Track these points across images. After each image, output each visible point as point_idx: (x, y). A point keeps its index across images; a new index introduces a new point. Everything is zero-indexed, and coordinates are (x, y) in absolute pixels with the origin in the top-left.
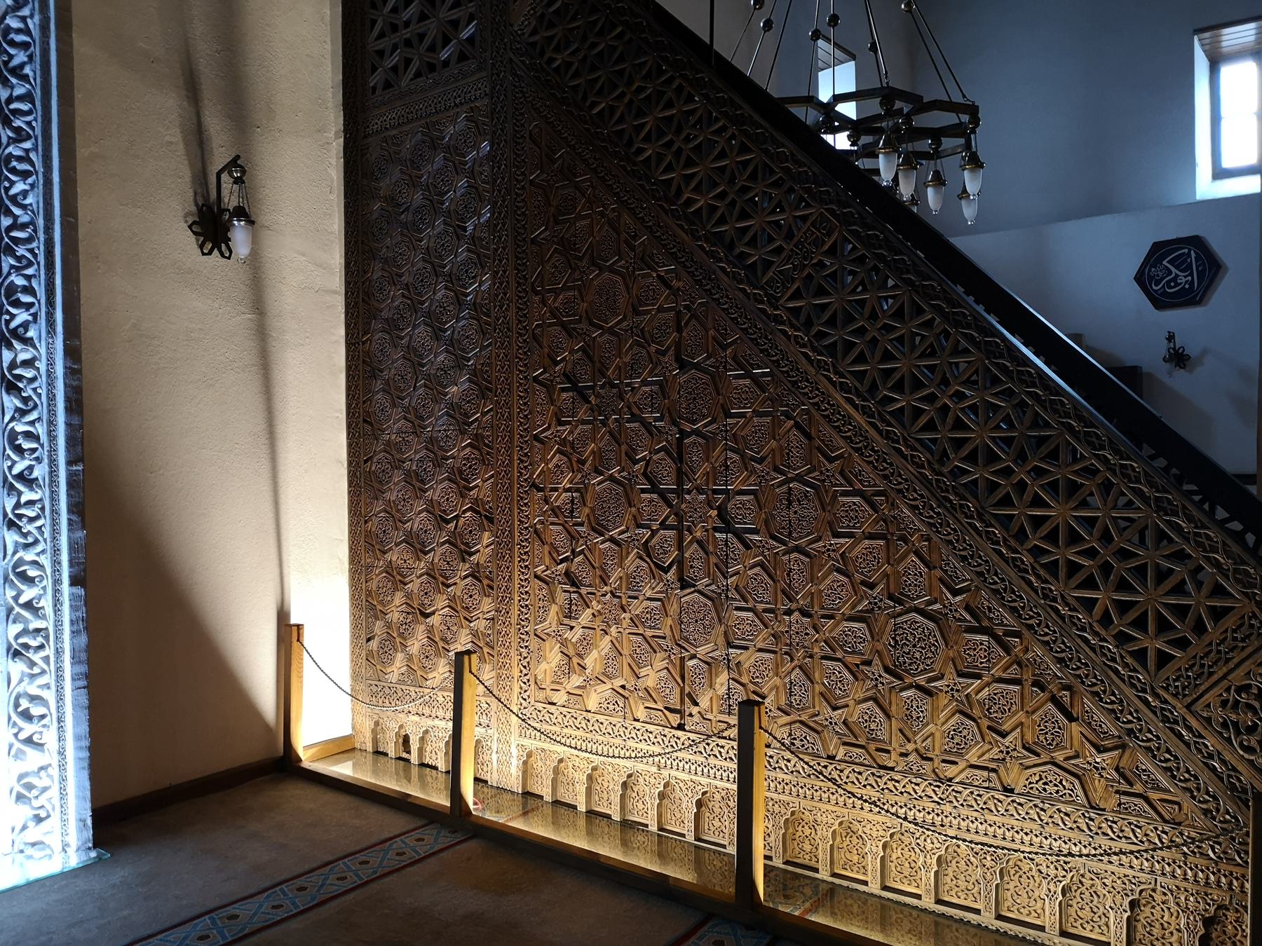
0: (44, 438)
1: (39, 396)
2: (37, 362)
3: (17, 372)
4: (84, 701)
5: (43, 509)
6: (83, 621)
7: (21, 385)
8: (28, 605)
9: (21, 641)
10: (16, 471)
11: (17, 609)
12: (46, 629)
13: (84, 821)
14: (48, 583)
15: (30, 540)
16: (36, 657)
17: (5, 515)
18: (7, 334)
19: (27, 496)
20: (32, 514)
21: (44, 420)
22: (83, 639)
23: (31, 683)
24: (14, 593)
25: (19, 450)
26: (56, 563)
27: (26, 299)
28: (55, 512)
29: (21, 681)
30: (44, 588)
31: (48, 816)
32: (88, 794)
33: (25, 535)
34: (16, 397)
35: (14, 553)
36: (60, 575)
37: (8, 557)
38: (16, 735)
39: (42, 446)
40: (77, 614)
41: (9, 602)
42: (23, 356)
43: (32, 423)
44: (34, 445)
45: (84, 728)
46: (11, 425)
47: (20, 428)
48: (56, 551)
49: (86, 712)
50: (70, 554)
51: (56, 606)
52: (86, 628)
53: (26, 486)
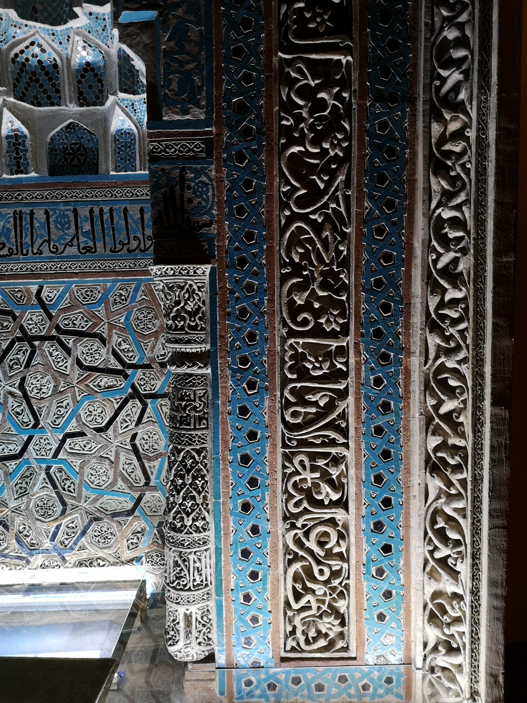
0: (471, 224)
1: (467, 172)
2: (468, 130)
3: (447, 147)
4: (503, 543)
5: (466, 310)
6: (505, 448)
7: (449, 163)
8: (448, 417)
9: (439, 454)
10: (440, 265)
11: (437, 420)
12: (465, 448)
13: (496, 682)
14: (468, 396)
15: (453, 345)
16: (455, 478)
17: (428, 314)
18: (437, 104)
19: (452, 294)
20: (455, 315)
21: (472, 201)
22: (505, 471)
23: (447, 503)
24: (434, 402)
25: (445, 241)
26: (478, 375)
28: (480, 314)
29: (438, 497)
30: (464, 402)
31: (458, 650)
32: (502, 648)
33: (447, 339)
34: (444, 178)
35: (437, 358)
36: (482, 390)
37: (430, 362)
38: (431, 552)
39: (468, 233)
40: (499, 440)
41: (429, 410)
42: (454, 126)
43: (458, 207)
44: (461, 234)
45: (500, 574)
46: (438, 212)
47: (447, 214)
48: (479, 362)
49: (504, 556)
50: (493, 366)
51: (476, 426)
52: (508, 458)
53: (449, 283)
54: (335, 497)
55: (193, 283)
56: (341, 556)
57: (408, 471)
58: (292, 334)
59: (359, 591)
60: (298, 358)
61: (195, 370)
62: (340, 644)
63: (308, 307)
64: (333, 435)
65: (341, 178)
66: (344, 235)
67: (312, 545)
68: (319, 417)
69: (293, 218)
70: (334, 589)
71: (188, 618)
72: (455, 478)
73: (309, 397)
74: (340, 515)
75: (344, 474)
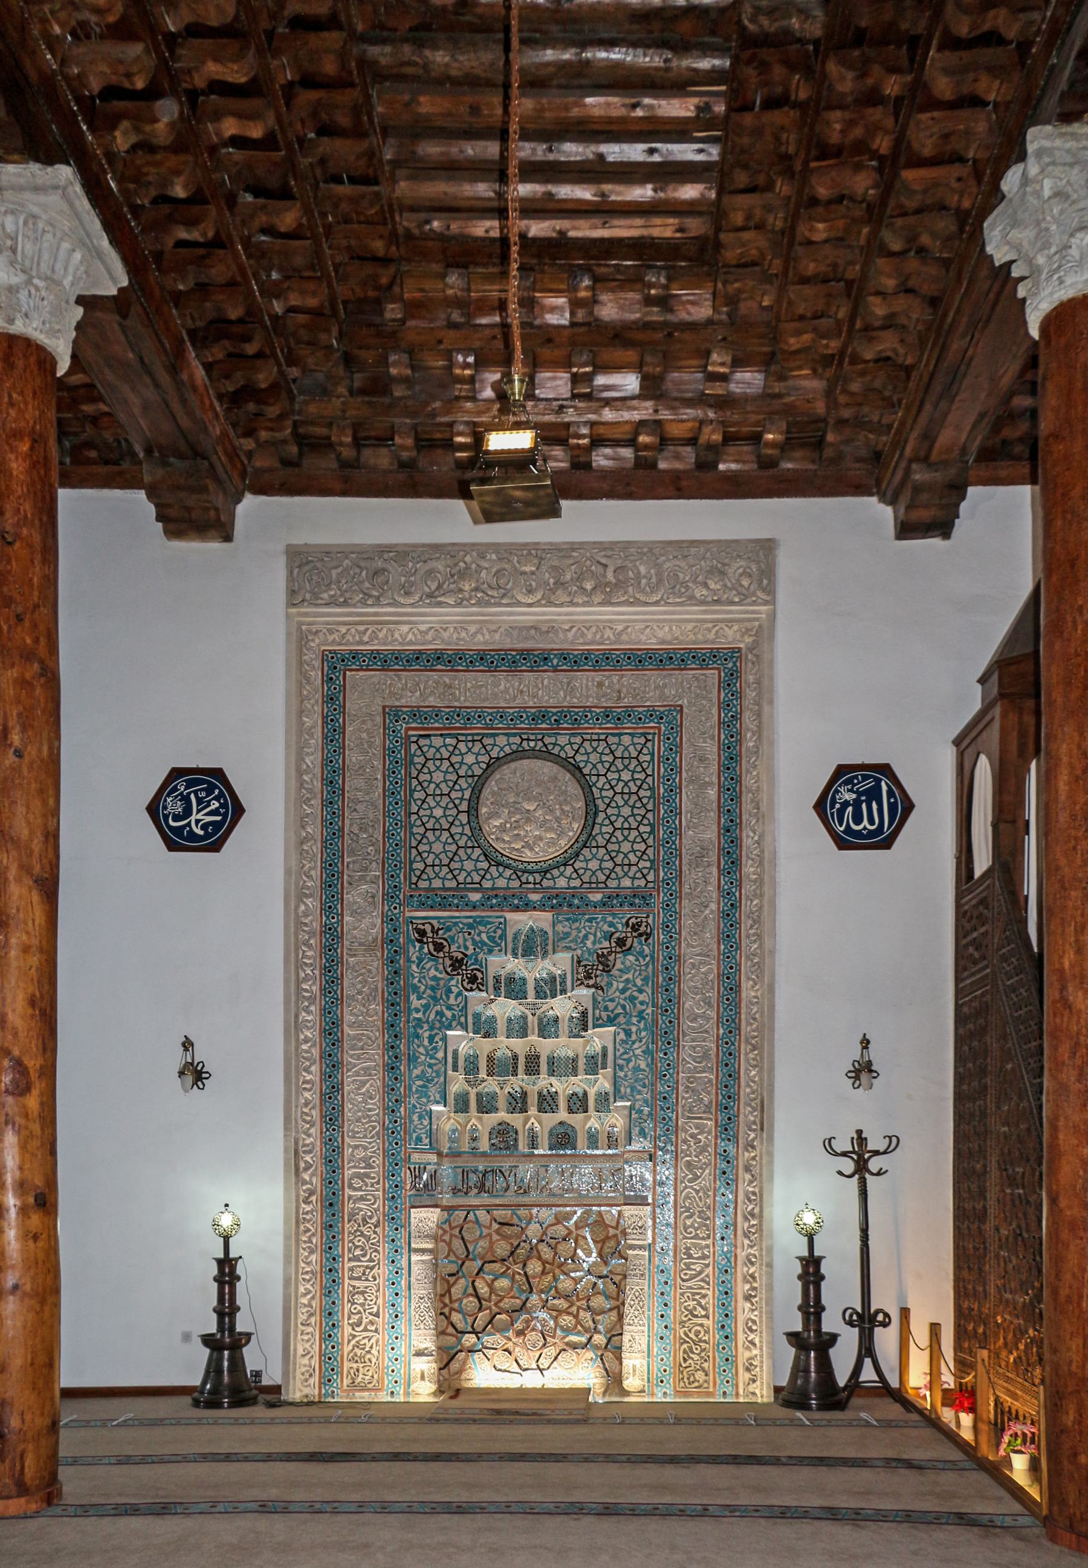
19: (753, 1222)
27: (754, 1127)
54: (703, 1313)
55: (642, 1214)
56: (705, 1342)
57: (736, 1301)
58: (686, 1238)
59: (714, 1358)
60: (688, 1249)
61: (641, 1253)
62: (706, 1385)
63: (692, 1226)
64: (702, 1284)
65: (707, 1171)
66: (709, 1196)
67: (692, 1335)
68: (696, 1276)
69: (686, 1187)
70: (702, 1358)
71: (634, 1366)
72: (754, 1300)
73: (693, 1267)
74: (705, 1321)
75: (708, 1303)
